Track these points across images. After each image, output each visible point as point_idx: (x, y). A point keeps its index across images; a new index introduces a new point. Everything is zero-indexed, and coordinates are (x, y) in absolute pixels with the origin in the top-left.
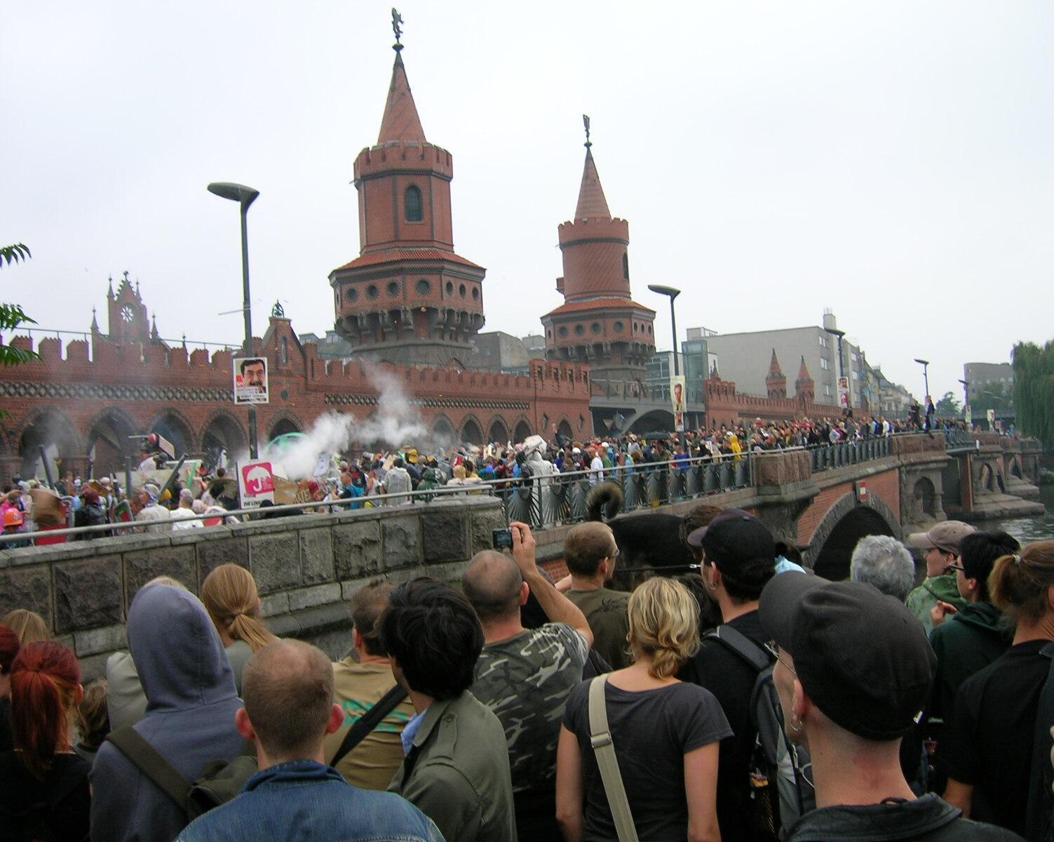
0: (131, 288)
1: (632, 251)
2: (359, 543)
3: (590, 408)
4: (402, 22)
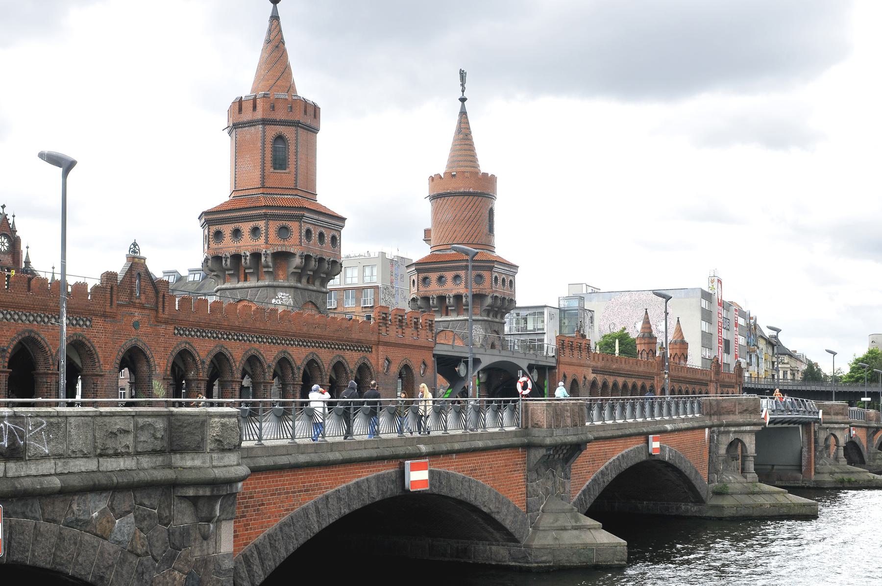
1: (499, 206)
2: (115, 431)
3: (434, 355)
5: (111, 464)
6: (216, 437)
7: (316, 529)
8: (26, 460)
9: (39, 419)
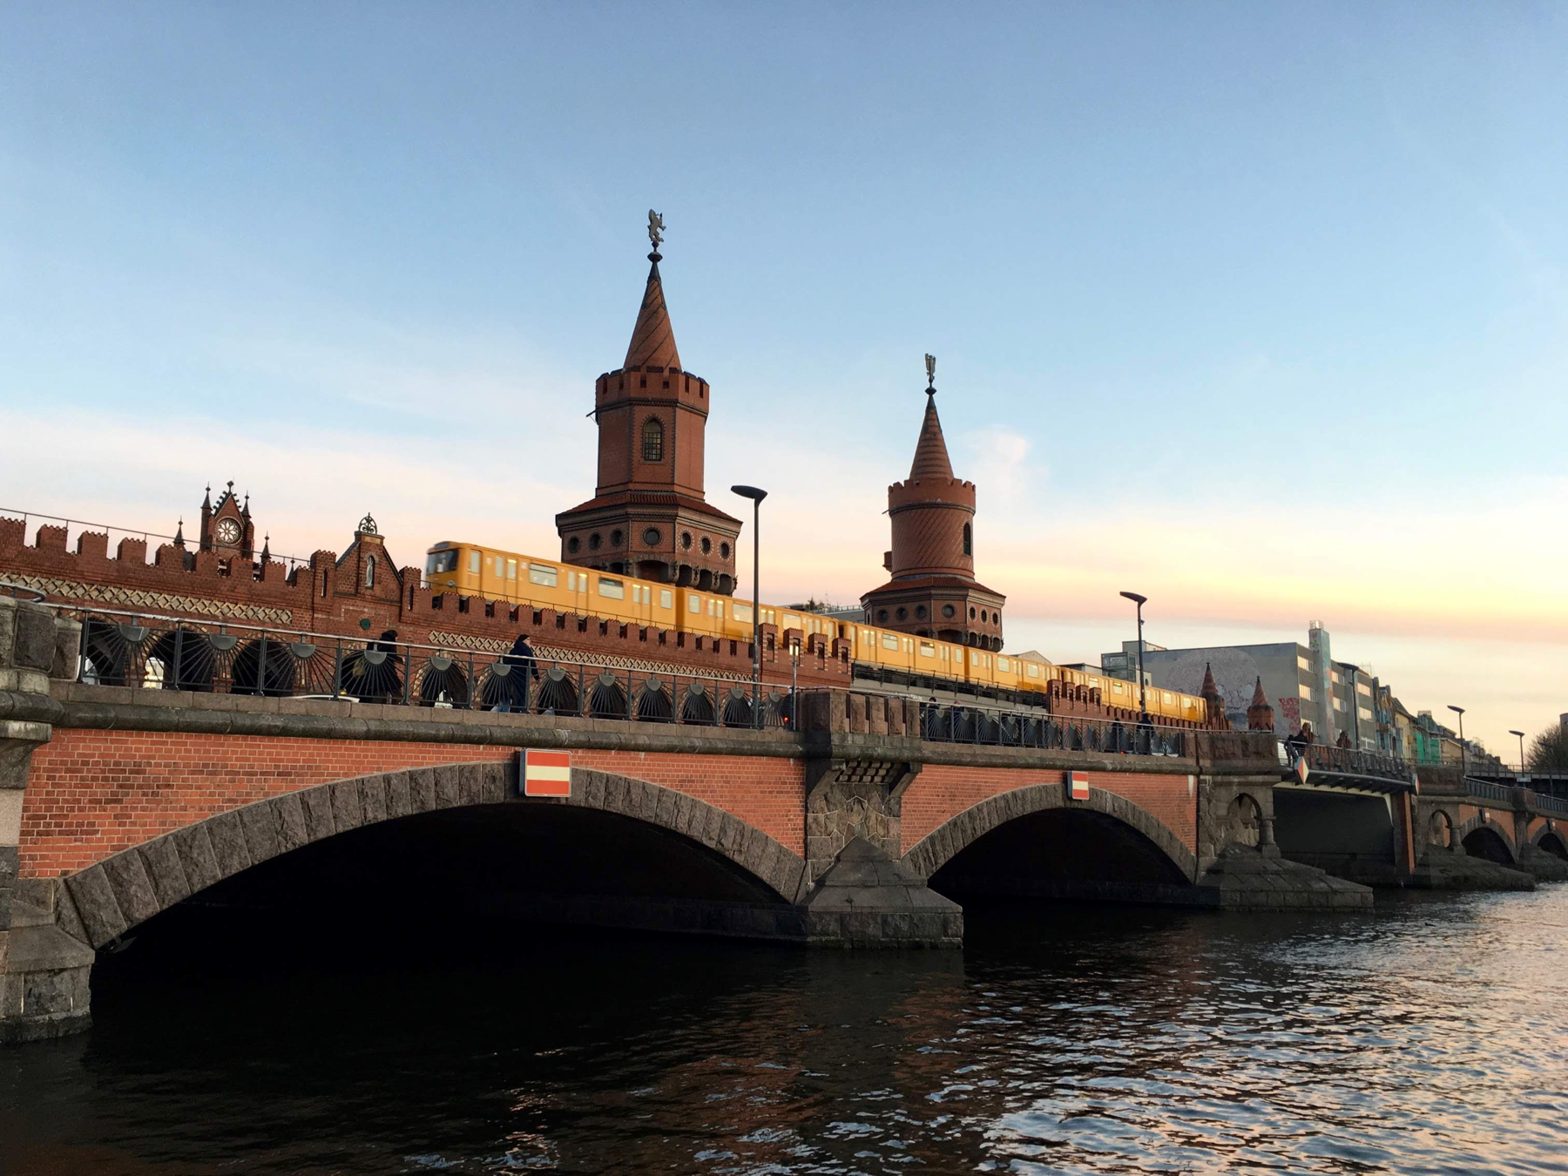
0: (235, 502)
4: (663, 229)
7: (302, 837)
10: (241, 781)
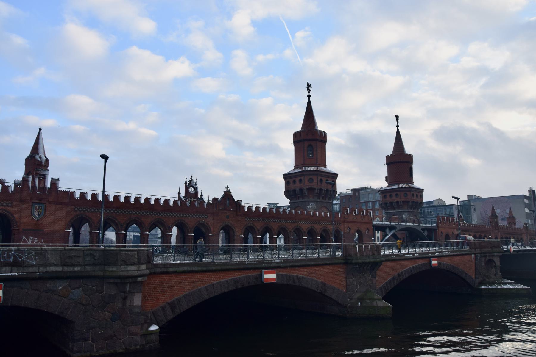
3: (373, 226)
4: (311, 87)
5: (66, 269)
6: (123, 259)
7: (206, 297)
8: (24, 267)
9: (31, 251)
10: (191, 284)
